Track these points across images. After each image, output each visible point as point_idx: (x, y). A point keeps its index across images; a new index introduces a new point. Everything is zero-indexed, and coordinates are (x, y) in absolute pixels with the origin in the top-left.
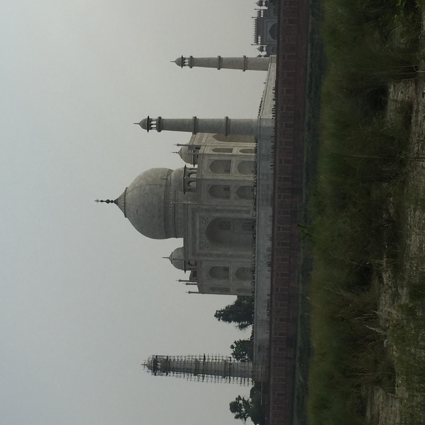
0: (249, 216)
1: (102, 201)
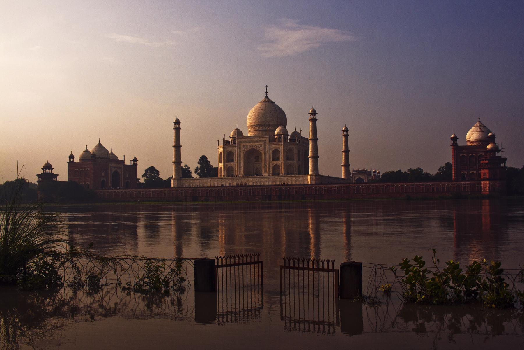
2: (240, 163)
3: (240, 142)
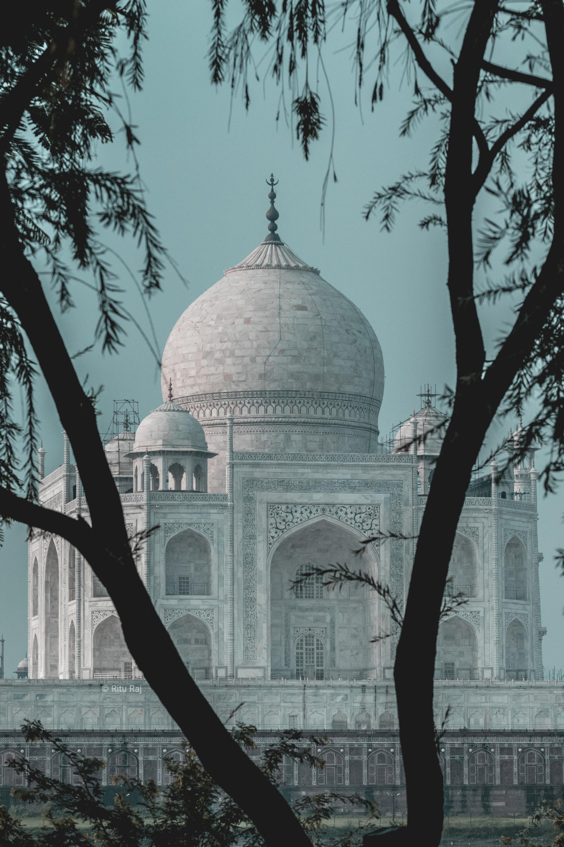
1: (273, 196)
2: (250, 602)
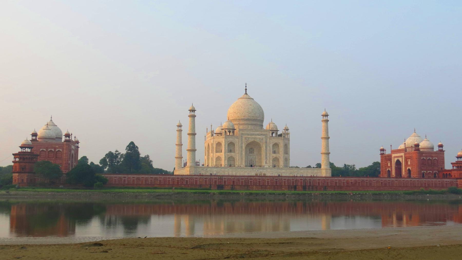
0: (264, 164)
2: (242, 154)
3: (242, 134)
